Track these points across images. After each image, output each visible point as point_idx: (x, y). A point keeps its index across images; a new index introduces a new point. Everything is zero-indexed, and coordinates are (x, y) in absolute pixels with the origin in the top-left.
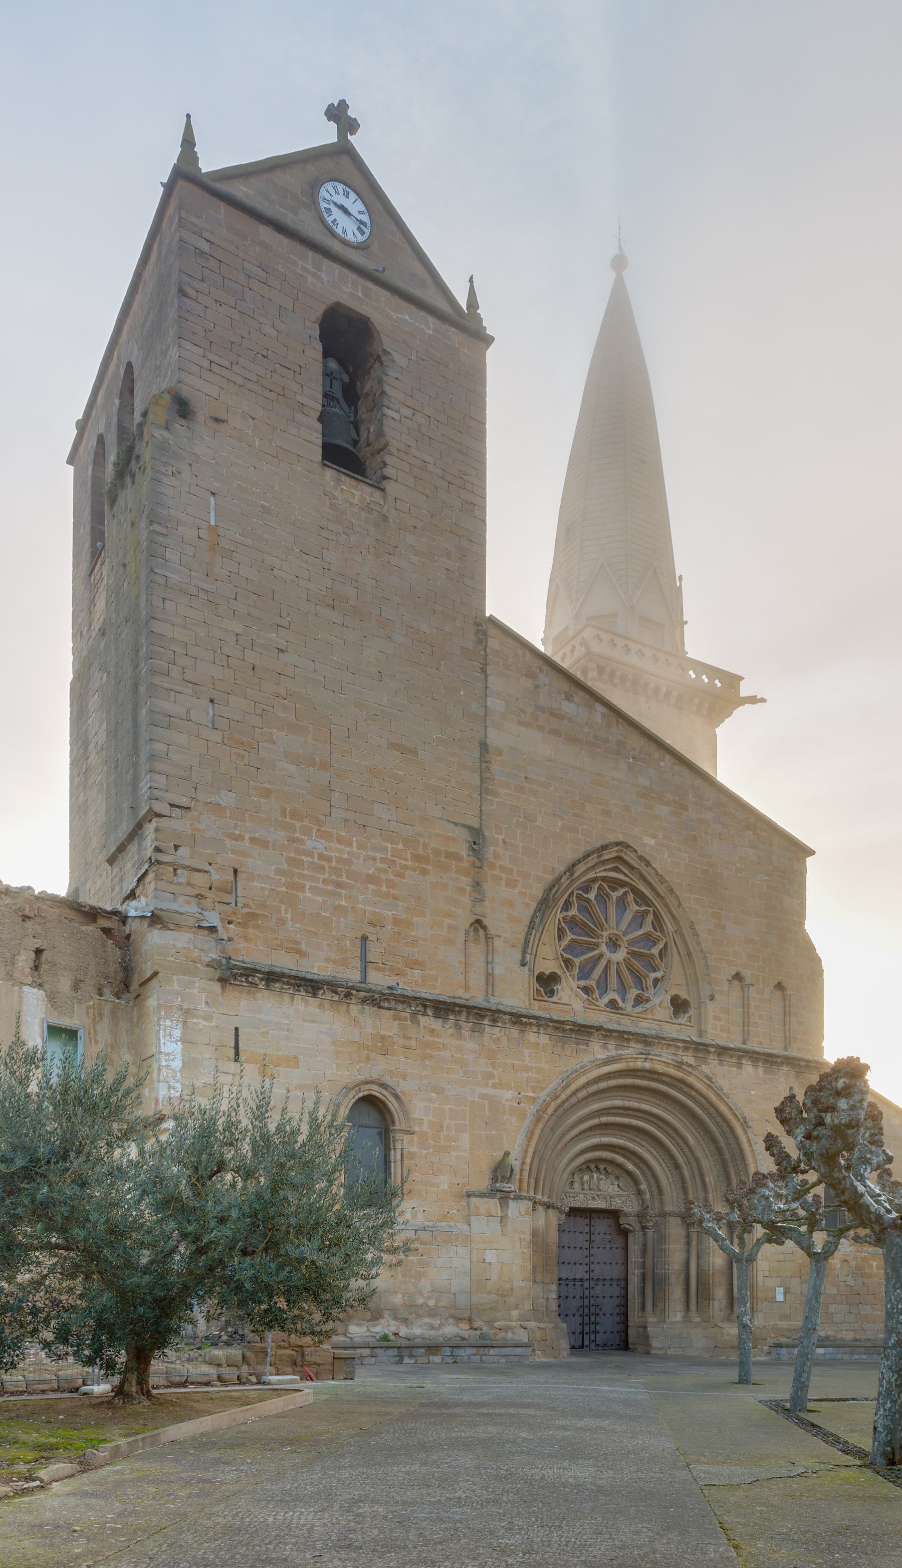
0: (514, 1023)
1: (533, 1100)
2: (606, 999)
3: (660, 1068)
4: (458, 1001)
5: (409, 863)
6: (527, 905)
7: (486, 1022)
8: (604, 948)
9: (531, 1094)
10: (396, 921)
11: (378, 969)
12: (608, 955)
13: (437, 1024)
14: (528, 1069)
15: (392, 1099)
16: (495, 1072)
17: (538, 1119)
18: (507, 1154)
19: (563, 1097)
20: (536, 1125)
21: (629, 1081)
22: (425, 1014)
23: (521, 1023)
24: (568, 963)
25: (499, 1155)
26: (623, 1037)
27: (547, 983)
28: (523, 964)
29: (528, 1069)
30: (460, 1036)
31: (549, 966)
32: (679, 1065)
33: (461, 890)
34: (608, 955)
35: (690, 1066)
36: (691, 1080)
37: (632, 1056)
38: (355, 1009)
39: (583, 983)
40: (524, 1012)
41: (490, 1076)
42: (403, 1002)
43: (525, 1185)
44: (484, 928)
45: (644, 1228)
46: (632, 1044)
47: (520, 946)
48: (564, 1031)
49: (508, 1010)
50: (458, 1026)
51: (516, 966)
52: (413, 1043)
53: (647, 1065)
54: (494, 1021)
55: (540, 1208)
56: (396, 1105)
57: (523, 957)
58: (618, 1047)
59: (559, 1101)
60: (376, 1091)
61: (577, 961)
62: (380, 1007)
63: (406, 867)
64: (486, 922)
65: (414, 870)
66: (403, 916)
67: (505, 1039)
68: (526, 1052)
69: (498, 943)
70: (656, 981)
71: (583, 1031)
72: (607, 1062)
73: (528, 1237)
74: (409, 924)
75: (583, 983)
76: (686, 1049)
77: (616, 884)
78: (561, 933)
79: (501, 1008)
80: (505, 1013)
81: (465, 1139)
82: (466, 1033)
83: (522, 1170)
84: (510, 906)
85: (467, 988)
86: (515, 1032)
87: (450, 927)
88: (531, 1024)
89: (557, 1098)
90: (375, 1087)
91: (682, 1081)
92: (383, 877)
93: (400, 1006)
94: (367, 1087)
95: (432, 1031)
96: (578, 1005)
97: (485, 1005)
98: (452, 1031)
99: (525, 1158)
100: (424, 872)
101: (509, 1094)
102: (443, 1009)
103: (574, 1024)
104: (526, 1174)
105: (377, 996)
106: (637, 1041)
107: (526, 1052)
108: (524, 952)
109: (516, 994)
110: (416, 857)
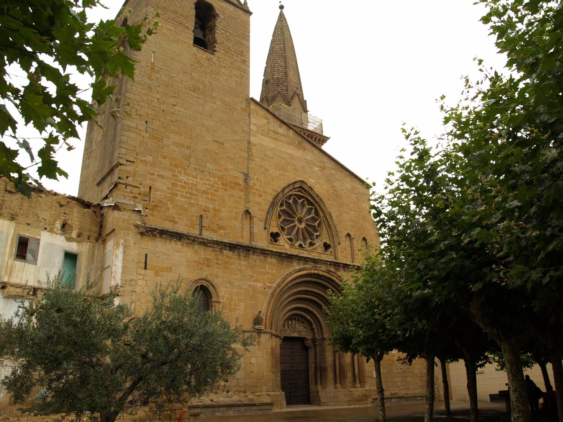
0: (262, 254)
1: (270, 287)
2: (297, 244)
3: (320, 273)
4: (239, 244)
5: (220, 186)
6: (266, 204)
7: (251, 253)
8: (296, 223)
9: (269, 285)
10: (214, 210)
11: (206, 230)
12: (298, 225)
13: (230, 254)
14: (268, 273)
15: (211, 287)
16: (254, 275)
17: (272, 296)
18: (260, 312)
19: (283, 286)
20: (271, 299)
21: (308, 279)
22: (225, 249)
23: (266, 254)
24: (283, 228)
25: (257, 312)
26: (306, 260)
27: (275, 237)
28: (265, 229)
29: (268, 273)
30: (240, 259)
31: (275, 230)
32: (328, 272)
33: (240, 198)
34: (298, 225)
35: (333, 272)
36: (333, 278)
37: (309, 268)
38: (196, 247)
39: (288, 237)
40: (266, 248)
41: (253, 277)
42: (216, 244)
43: (267, 326)
44: (249, 213)
45: (315, 346)
46: (309, 263)
47: (264, 220)
48: (282, 257)
49: (259, 247)
50: (239, 255)
51: (262, 229)
52: (220, 262)
53: (316, 272)
54: (254, 252)
55: (273, 337)
56: (213, 290)
57: (265, 225)
58: (304, 264)
59: (281, 288)
60: (204, 283)
61: (286, 227)
62: (207, 246)
63: (219, 188)
64: (250, 211)
65: (222, 189)
66: (217, 207)
67: (258, 260)
68: (267, 266)
69: (255, 219)
70: (317, 236)
71: (290, 257)
72: (300, 270)
73: (270, 351)
74: (219, 211)
75: (288, 237)
76: (331, 265)
77: (300, 197)
78: (280, 216)
79: (257, 247)
80: (258, 249)
81: (242, 305)
82: (242, 258)
83: (266, 319)
84: (260, 205)
85: (242, 238)
86: (262, 258)
87: (236, 213)
88: (269, 254)
89: (280, 286)
90: (204, 282)
91: (330, 279)
92: (210, 191)
93: (215, 246)
94: (201, 281)
95: (228, 257)
96: (287, 246)
97: (250, 245)
98: (236, 257)
99: (267, 314)
100: (226, 190)
101: (260, 285)
102: (233, 247)
103: (286, 254)
104: (268, 321)
105: (206, 241)
106: (312, 262)
107: (267, 266)
108: (265, 224)
109: (262, 242)
110: (222, 184)
